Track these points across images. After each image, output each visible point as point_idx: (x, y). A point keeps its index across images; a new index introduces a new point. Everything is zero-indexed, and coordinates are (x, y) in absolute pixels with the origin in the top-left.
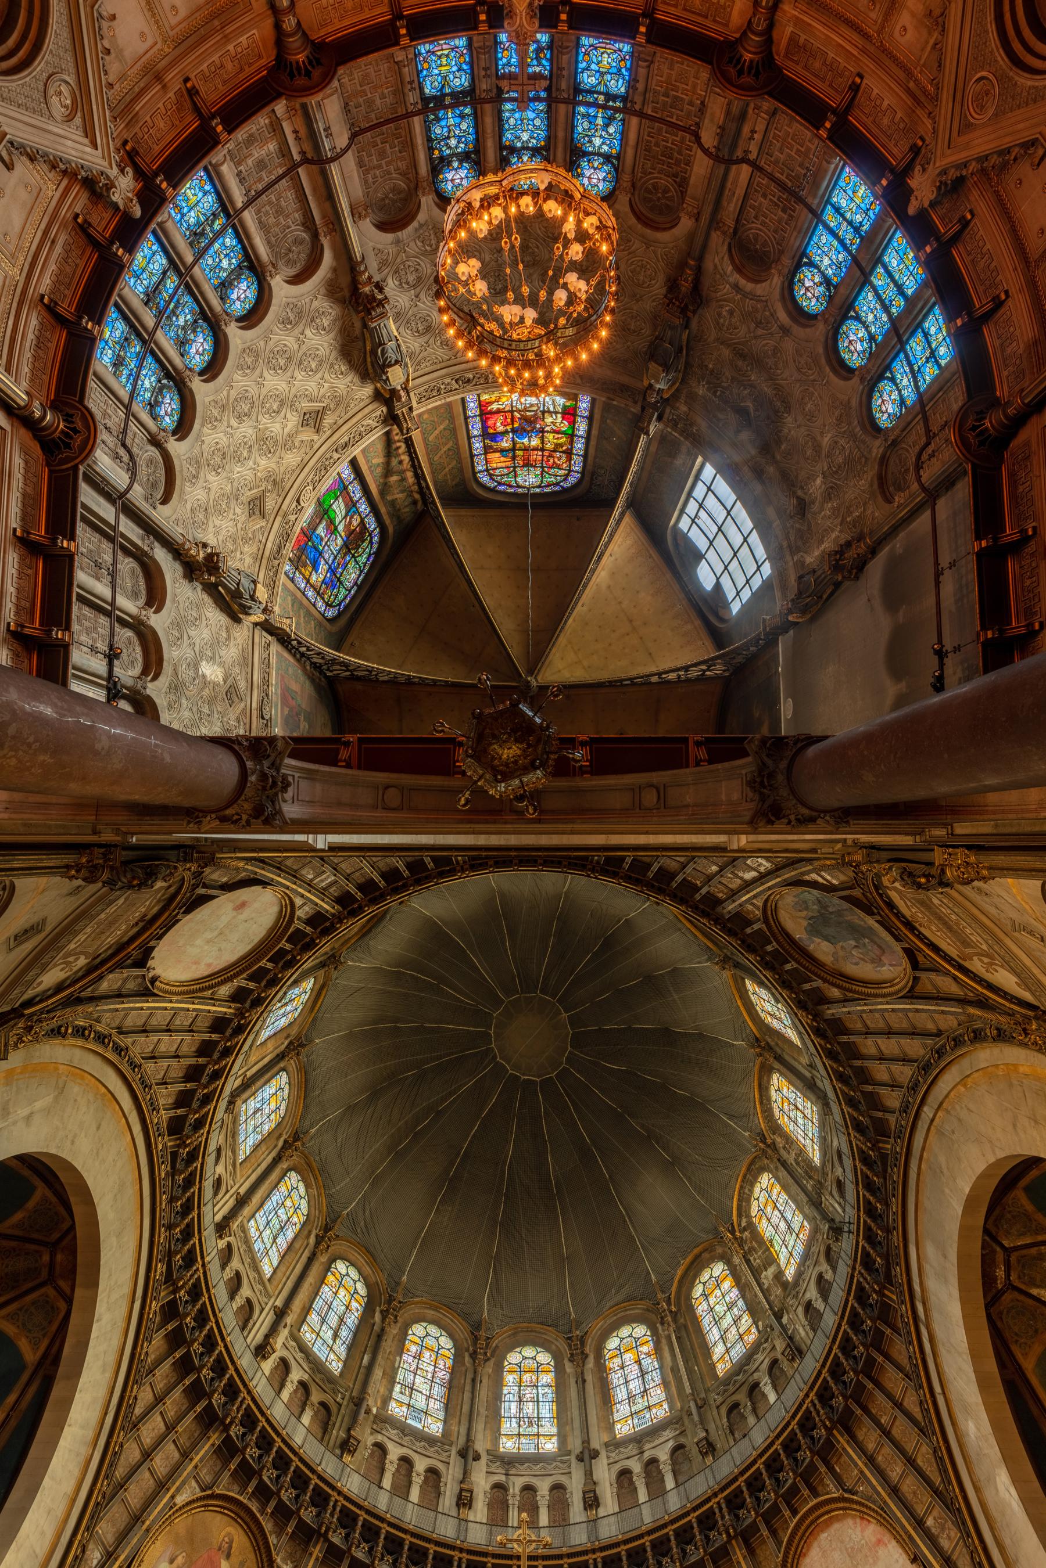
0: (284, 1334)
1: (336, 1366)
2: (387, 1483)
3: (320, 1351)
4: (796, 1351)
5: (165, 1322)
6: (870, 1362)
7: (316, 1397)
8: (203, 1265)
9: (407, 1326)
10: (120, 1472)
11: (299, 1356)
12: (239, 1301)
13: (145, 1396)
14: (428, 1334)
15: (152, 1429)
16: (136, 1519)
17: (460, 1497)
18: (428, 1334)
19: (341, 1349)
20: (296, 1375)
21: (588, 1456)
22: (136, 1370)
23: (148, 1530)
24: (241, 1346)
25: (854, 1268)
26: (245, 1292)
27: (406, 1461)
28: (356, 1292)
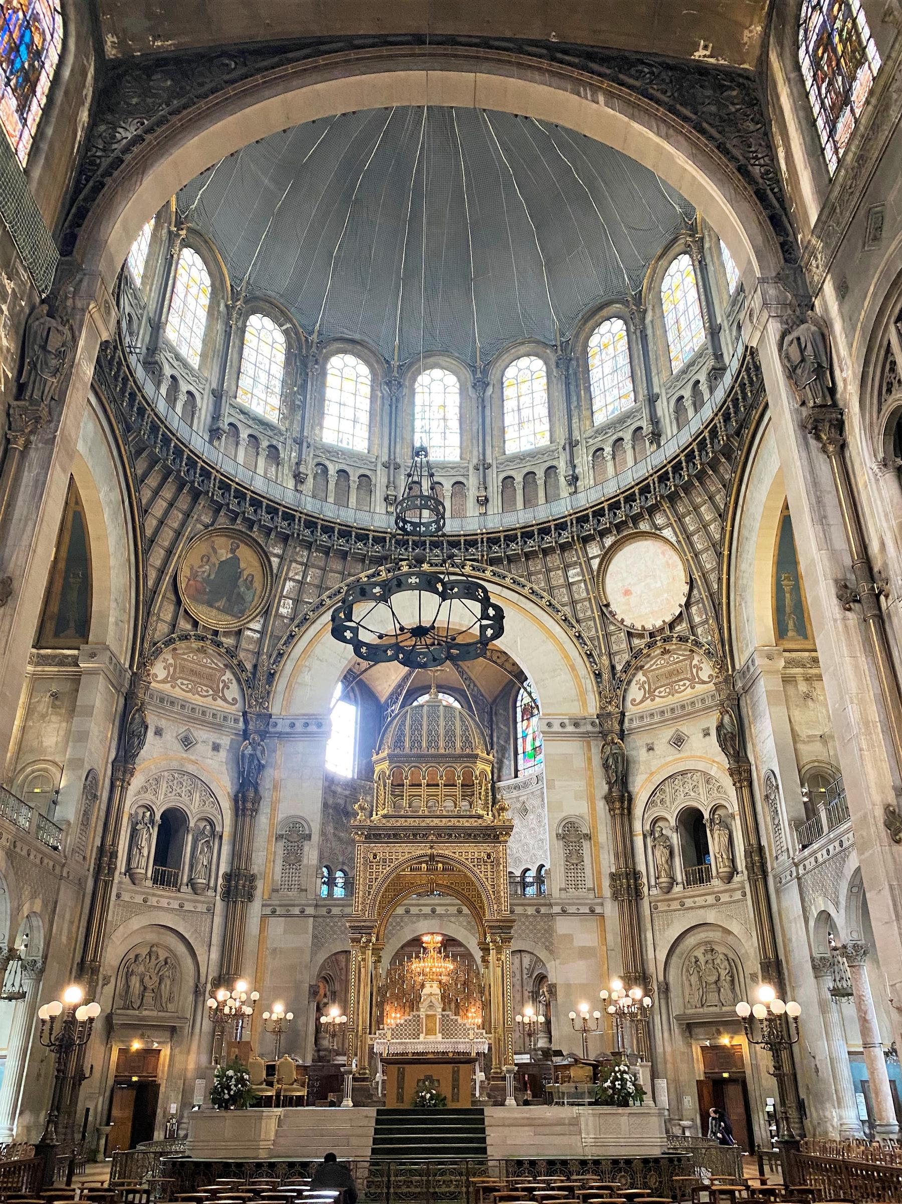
0: (226, 410)
1: (273, 417)
2: (331, 500)
3: (257, 409)
4: (656, 437)
5: (139, 453)
6: (703, 472)
7: (265, 444)
8: (152, 410)
9: (327, 359)
10: (149, 532)
11: (242, 417)
12: (182, 398)
13: (146, 495)
14: (346, 365)
15: (159, 507)
16: (170, 552)
17: (386, 499)
18: (346, 365)
19: (275, 401)
20: (244, 434)
21: (484, 467)
22: (131, 486)
23: (179, 557)
24: (198, 443)
25: (716, 415)
26: (184, 387)
27: (342, 473)
28: (274, 342)
